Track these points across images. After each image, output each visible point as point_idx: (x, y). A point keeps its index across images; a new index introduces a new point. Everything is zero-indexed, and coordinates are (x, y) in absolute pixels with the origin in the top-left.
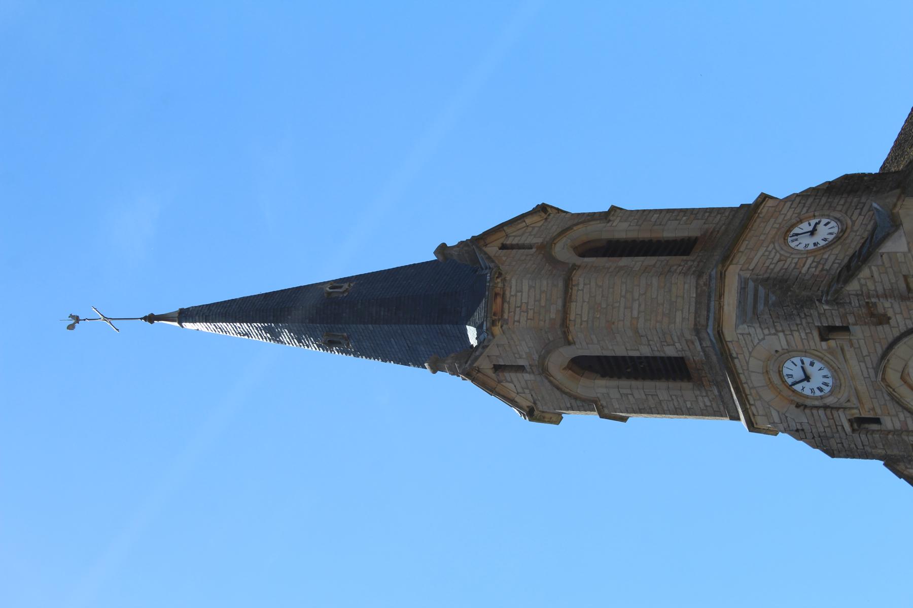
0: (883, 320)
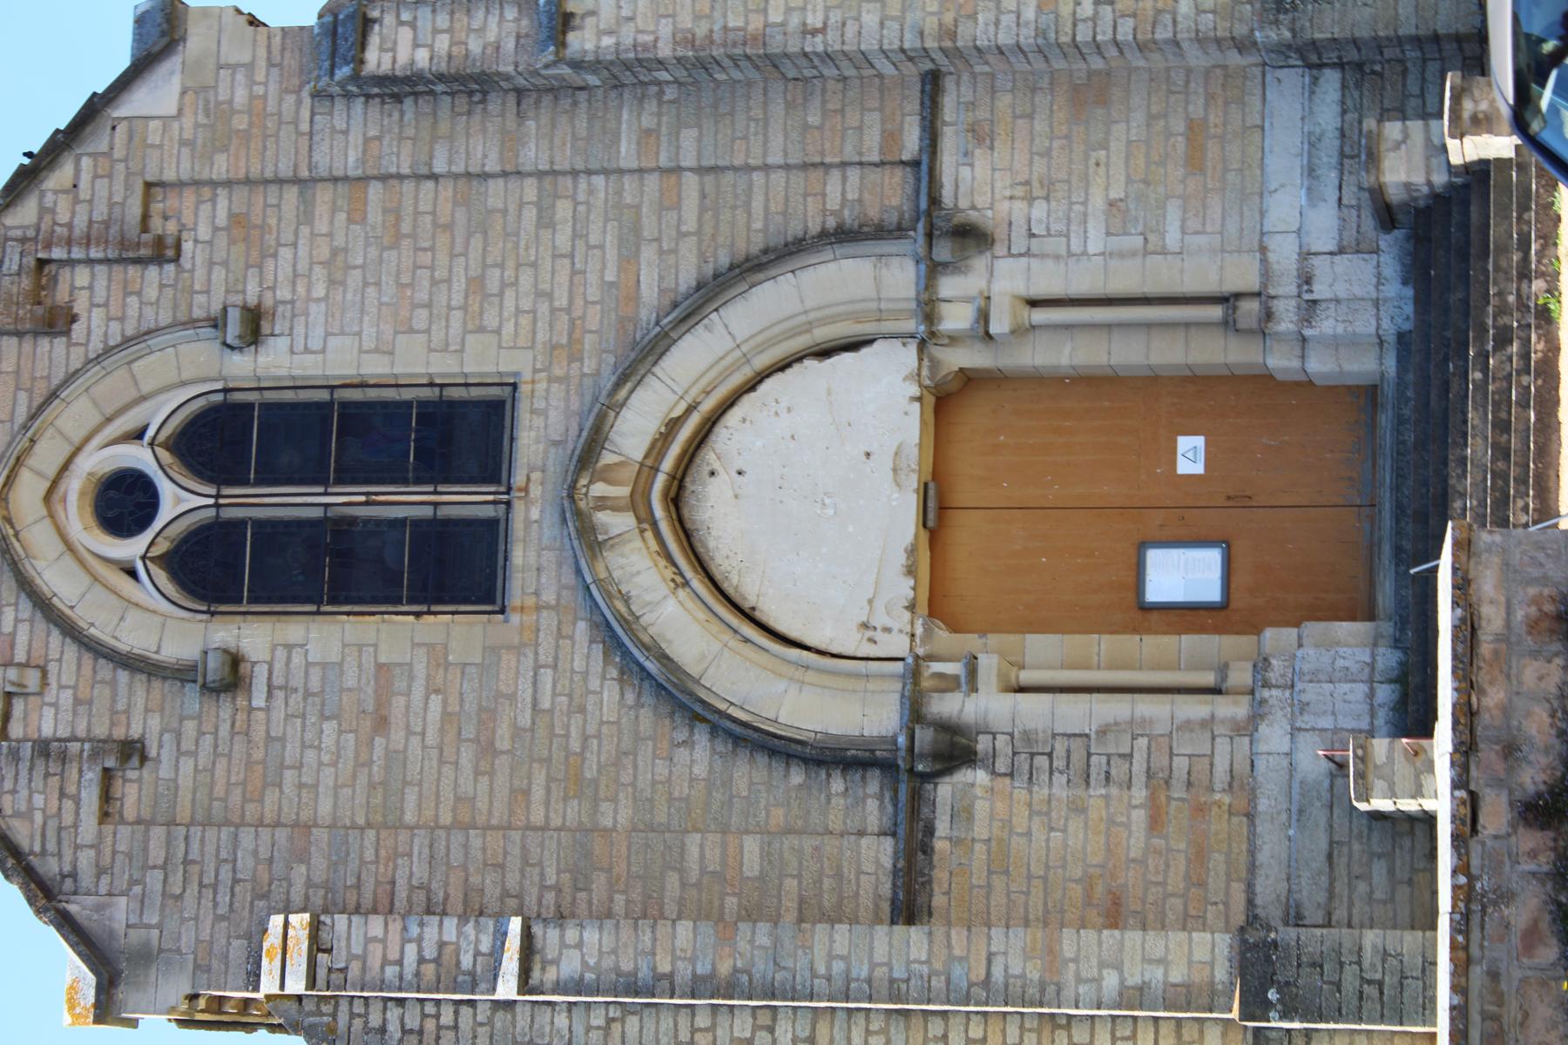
0: (58, 322)
